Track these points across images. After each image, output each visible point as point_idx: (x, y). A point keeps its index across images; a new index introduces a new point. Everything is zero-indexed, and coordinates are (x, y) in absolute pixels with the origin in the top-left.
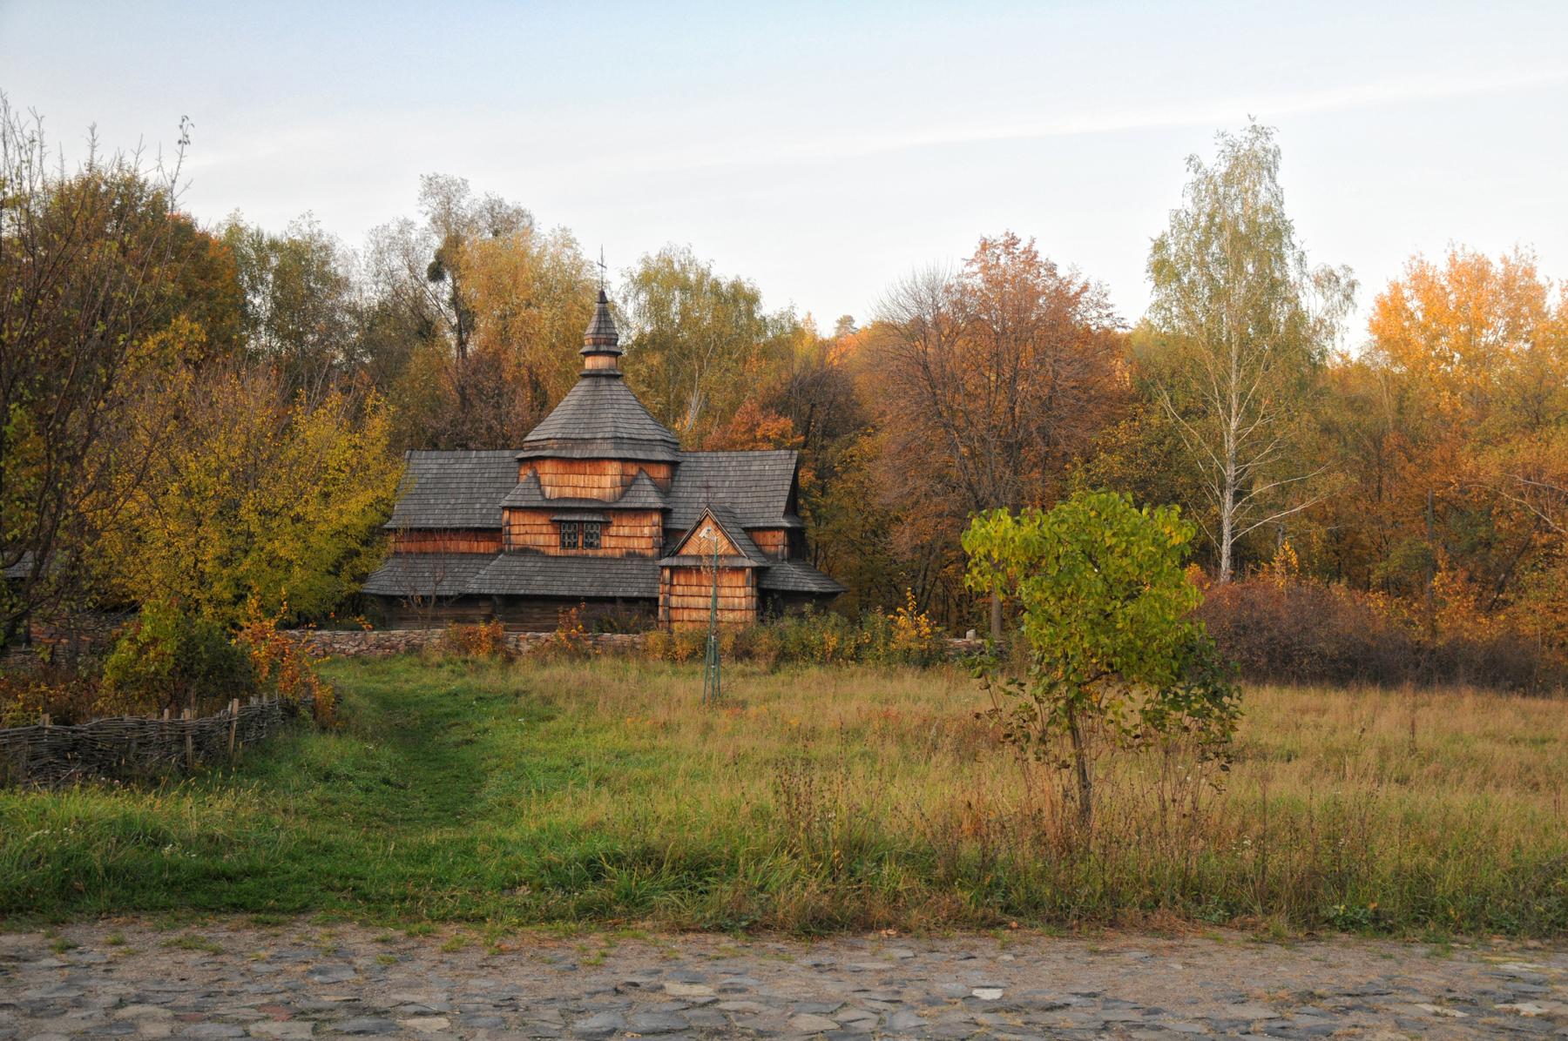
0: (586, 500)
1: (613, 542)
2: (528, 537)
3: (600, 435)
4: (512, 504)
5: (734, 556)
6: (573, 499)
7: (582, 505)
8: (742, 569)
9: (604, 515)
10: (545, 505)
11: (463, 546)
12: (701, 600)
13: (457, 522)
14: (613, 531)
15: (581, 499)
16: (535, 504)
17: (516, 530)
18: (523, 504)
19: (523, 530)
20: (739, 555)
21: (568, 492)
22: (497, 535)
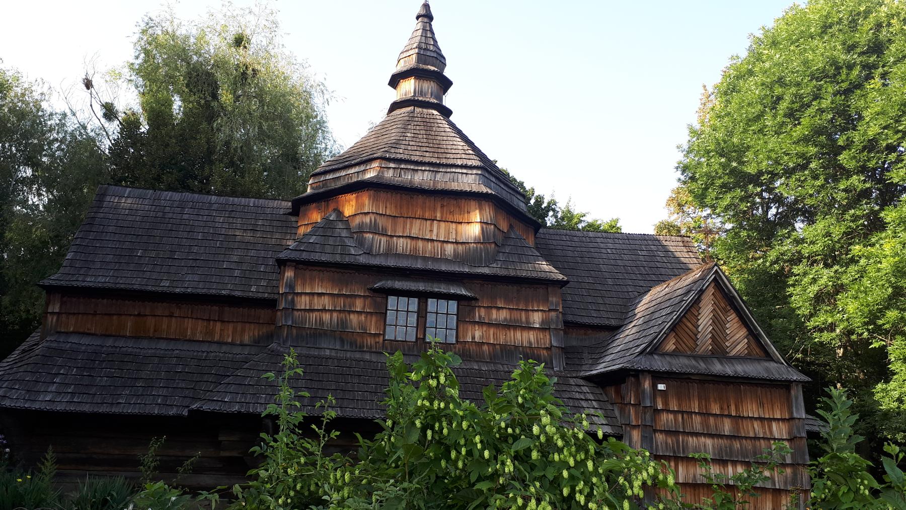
0: (434, 259)
1: (478, 333)
2: (326, 317)
3: (459, 162)
4: (305, 256)
5: (758, 360)
6: (414, 256)
7: (430, 266)
8: (786, 385)
9: (467, 289)
10: (363, 260)
11: (194, 328)
12: (709, 442)
13: (190, 283)
14: (480, 314)
15: (424, 258)
16: (347, 259)
17: (303, 302)
18: (324, 258)
19: (318, 303)
20: (768, 357)
21: (402, 245)
22: (264, 314)
